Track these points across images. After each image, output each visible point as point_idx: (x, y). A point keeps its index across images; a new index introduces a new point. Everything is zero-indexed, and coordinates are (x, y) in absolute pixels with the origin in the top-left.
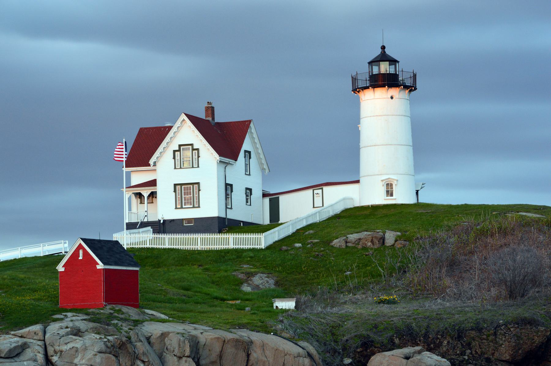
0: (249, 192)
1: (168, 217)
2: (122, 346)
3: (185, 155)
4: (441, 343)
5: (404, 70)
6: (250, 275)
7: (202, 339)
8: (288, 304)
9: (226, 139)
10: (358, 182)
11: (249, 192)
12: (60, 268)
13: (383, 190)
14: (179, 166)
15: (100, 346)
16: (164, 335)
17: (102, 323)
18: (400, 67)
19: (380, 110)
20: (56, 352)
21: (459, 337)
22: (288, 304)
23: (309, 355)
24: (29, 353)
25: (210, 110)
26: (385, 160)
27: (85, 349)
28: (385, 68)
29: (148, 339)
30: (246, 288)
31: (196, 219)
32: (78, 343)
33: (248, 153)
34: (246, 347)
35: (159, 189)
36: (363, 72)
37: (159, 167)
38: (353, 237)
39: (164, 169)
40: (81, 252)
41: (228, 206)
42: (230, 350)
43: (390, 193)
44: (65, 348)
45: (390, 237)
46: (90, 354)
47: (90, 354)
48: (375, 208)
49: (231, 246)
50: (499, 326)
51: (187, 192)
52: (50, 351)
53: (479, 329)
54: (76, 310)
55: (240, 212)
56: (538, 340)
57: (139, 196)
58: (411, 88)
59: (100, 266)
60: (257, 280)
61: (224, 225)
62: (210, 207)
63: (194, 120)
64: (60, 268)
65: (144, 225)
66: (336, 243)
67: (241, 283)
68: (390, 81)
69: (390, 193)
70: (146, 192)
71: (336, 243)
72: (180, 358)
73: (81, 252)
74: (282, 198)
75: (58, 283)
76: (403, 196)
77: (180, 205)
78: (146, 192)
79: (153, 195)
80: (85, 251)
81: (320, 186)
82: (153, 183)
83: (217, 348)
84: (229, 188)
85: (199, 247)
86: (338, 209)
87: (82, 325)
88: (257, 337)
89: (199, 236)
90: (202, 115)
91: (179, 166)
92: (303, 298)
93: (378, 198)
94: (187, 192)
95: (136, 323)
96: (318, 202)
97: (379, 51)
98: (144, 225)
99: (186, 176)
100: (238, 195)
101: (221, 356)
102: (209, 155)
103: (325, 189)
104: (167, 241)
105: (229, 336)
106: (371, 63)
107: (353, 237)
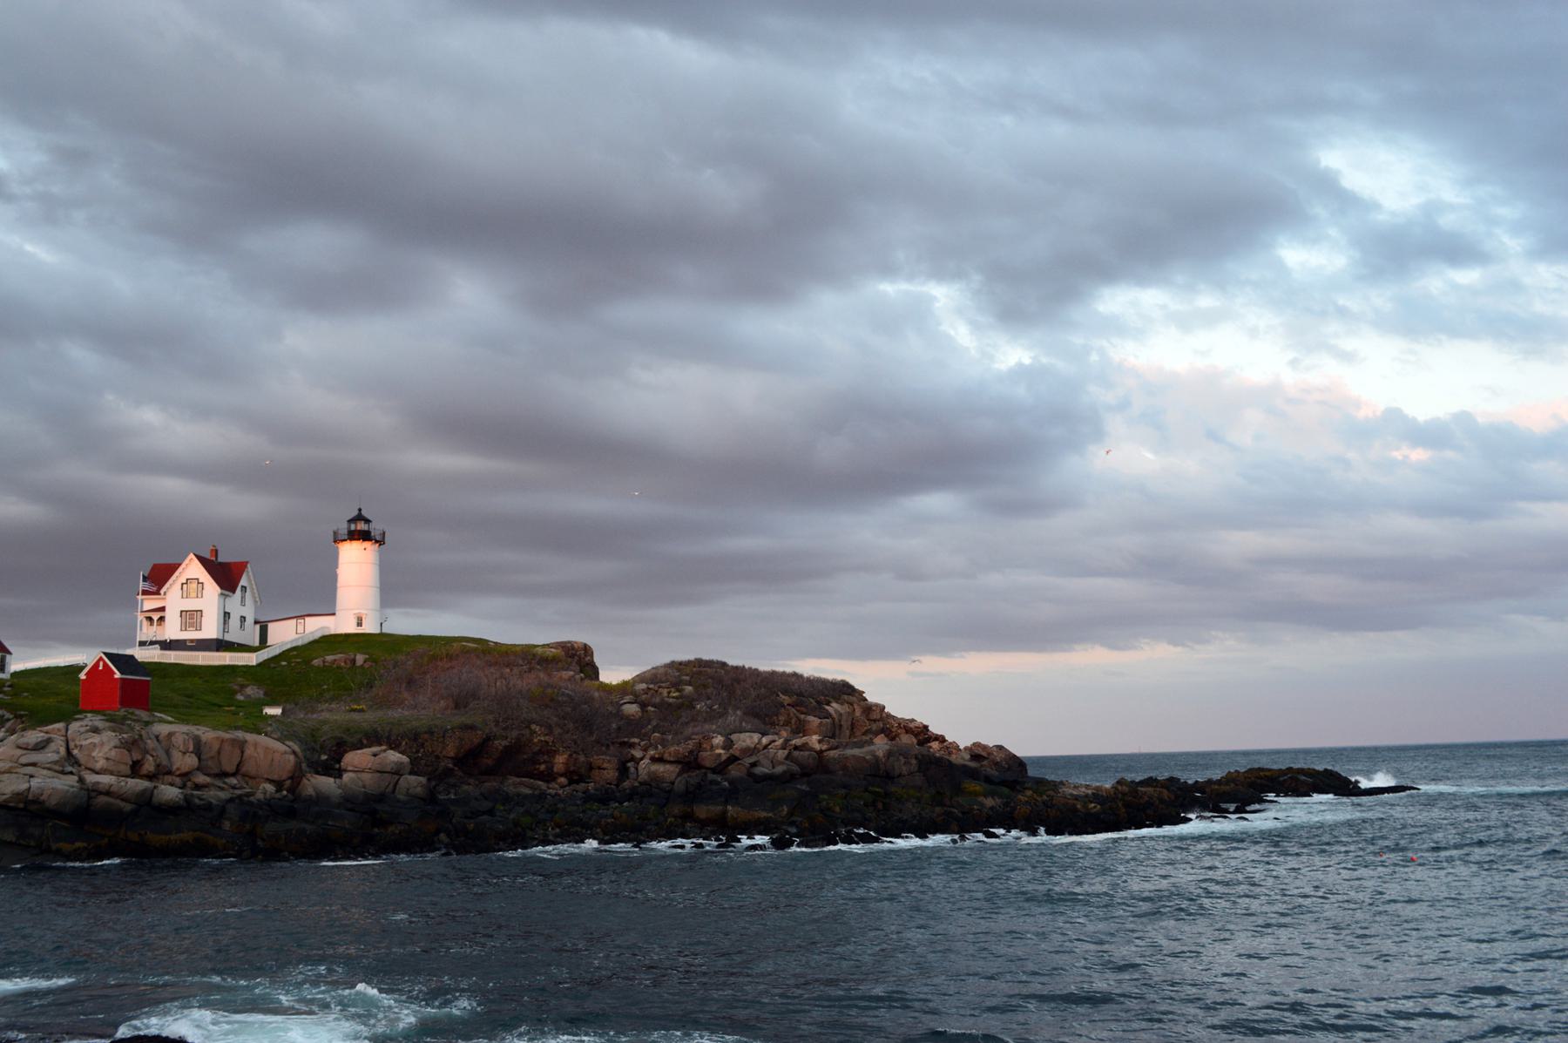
0: (243, 619)
1: (174, 637)
2: (134, 742)
5: (375, 528)
6: (243, 687)
7: (204, 738)
8: (275, 711)
9: (226, 575)
11: (243, 619)
12: (82, 676)
13: (355, 622)
14: (185, 595)
15: (115, 742)
16: (170, 735)
17: (117, 723)
18: (372, 526)
19: (356, 561)
21: (415, 739)
22: (277, 711)
23: (294, 753)
24: (53, 746)
26: (357, 596)
27: (102, 744)
28: (361, 526)
29: (157, 737)
30: (240, 697)
32: (96, 739)
33: (244, 588)
34: (242, 745)
36: (343, 528)
37: (169, 596)
38: (329, 658)
39: (174, 598)
41: (225, 630)
42: (227, 747)
43: (360, 624)
45: (360, 659)
46: (106, 748)
47: (106, 748)
48: (347, 636)
51: (191, 618)
52: (72, 745)
53: (432, 733)
54: (95, 712)
55: (233, 636)
56: (476, 741)
57: (150, 619)
58: (380, 542)
59: (118, 675)
60: (249, 691)
61: (220, 645)
62: (210, 630)
63: (202, 560)
64: (82, 676)
65: (152, 643)
66: (316, 662)
67: (235, 692)
69: (360, 624)
70: (156, 617)
71: (316, 662)
75: (79, 689)
76: (370, 627)
77: (184, 628)
78: (156, 617)
79: (162, 619)
81: (302, 617)
82: (163, 609)
83: (216, 747)
84: (227, 615)
85: (200, 662)
86: (317, 636)
87: (100, 724)
88: (250, 737)
89: (201, 654)
90: (207, 555)
91: (185, 595)
93: (350, 628)
95: (147, 723)
96: (300, 629)
97: (356, 513)
98: (152, 643)
100: (234, 622)
101: (219, 753)
102: (212, 588)
104: (173, 657)
105: (227, 736)
106: (350, 521)
107: (329, 658)
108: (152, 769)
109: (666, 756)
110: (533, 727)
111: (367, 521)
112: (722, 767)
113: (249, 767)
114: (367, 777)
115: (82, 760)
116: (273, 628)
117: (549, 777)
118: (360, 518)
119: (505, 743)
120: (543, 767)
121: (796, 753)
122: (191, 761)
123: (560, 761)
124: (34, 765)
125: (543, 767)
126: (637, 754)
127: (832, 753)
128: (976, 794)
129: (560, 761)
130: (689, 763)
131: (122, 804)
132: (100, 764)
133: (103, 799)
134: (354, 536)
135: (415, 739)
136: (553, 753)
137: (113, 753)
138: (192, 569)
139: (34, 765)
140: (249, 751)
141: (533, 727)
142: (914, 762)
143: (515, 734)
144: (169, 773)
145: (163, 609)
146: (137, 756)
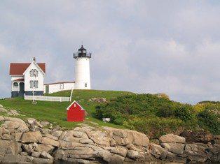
3: (34, 73)
12: (68, 109)
25: (34, 59)
43: (86, 86)
45: (104, 100)
61: (47, 94)
62: (41, 88)
64: (68, 109)
69: (86, 86)
75: (66, 113)
76: (89, 88)
81: (63, 83)
89: (51, 97)
94: (35, 83)
99: (33, 79)
117: (206, 142)
118: (82, 49)
132: (101, 143)
137: (105, 138)
140: (135, 136)
145: (23, 80)
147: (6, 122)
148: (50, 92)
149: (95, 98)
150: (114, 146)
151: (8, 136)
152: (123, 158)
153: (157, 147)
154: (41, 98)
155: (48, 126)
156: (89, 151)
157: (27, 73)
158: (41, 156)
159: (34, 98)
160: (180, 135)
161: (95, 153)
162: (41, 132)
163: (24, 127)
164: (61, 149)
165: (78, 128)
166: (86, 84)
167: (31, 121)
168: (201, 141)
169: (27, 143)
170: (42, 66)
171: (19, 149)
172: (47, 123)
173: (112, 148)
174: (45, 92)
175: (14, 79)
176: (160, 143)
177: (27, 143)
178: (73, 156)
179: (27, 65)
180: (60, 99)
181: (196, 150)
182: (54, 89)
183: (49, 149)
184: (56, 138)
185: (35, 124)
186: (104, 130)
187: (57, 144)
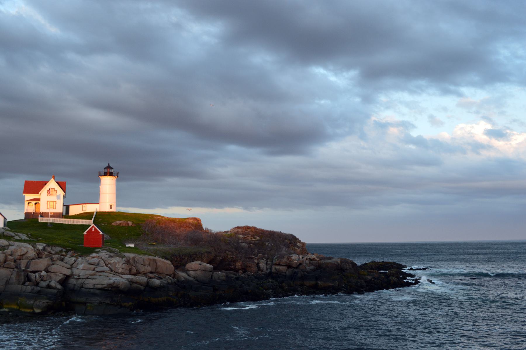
4: (185, 258)
10: (98, 204)
12: (85, 233)
15: (123, 262)
16: (134, 258)
20: (109, 263)
21: (191, 257)
31: (54, 213)
35: (41, 202)
38: (118, 222)
40: (93, 229)
43: (111, 208)
44: (112, 262)
45: (130, 223)
46: (121, 264)
49: (81, 224)
50: (202, 254)
52: (107, 263)
53: (196, 255)
56: (212, 257)
59: (101, 233)
62: (60, 209)
66: (113, 224)
68: (111, 174)
69: (111, 208)
71: (113, 224)
72: (144, 265)
73: (93, 229)
74: (71, 207)
76: (114, 210)
80: (95, 229)
82: (39, 200)
89: (70, 220)
92: (138, 243)
93: (107, 209)
96: (84, 209)
97: (107, 165)
103: (87, 205)
108: (136, 272)
109: (281, 263)
110: (227, 252)
111: (111, 168)
112: (297, 267)
113: (159, 270)
114: (199, 273)
115: (113, 269)
116: (71, 207)
118: (109, 167)
119: (221, 258)
120: (233, 267)
121: (312, 262)
122: (149, 269)
123: (239, 265)
124: (103, 272)
125: (233, 267)
126: (256, 262)
127: (321, 261)
128: (365, 275)
129: (239, 265)
130: (289, 266)
131: (141, 287)
133: (135, 285)
134: (106, 174)
135: (191, 257)
136: (236, 262)
137: (124, 266)
138: (52, 184)
139: (103, 272)
140: (159, 264)
141: (227, 252)
142: (351, 265)
143: (223, 255)
144: (140, 273)
146: (130, 267)
147: (12, 248)
148: (71, 213)
149: (121, 222)
150: (134, 275)
151: (13, 264)
152: (143, 288)
153: (182, 275)
154: (58, 221)
155: (61, 251)
156: (104, 281)
157: (44, 192)
158: (49, 286)
159: (50, 220)
160: (209, 263)
161: (111, 281)
162: (52, 259)
163: (32, 253)
164: (74, 278)
165: (94, 255)
166: (111, 206)
167: (40, 247)
168: (231, 269)
169: (34, 272)
170: (62, 185)
171: (22, 278)
172: (59, 249)
173: (133, 277)
174: (64, 214)
175: (29, 197)
176: (186, 271)
177: (34, 272)
178: (86, 286)
179: (45, 183)
180: (81, 222)
181: (224, 278)
182: (74, 210)
183: (60, 278)
184: (69, 266)
185: (44, 249)
186: (123, 257)
187: (68, 272)
